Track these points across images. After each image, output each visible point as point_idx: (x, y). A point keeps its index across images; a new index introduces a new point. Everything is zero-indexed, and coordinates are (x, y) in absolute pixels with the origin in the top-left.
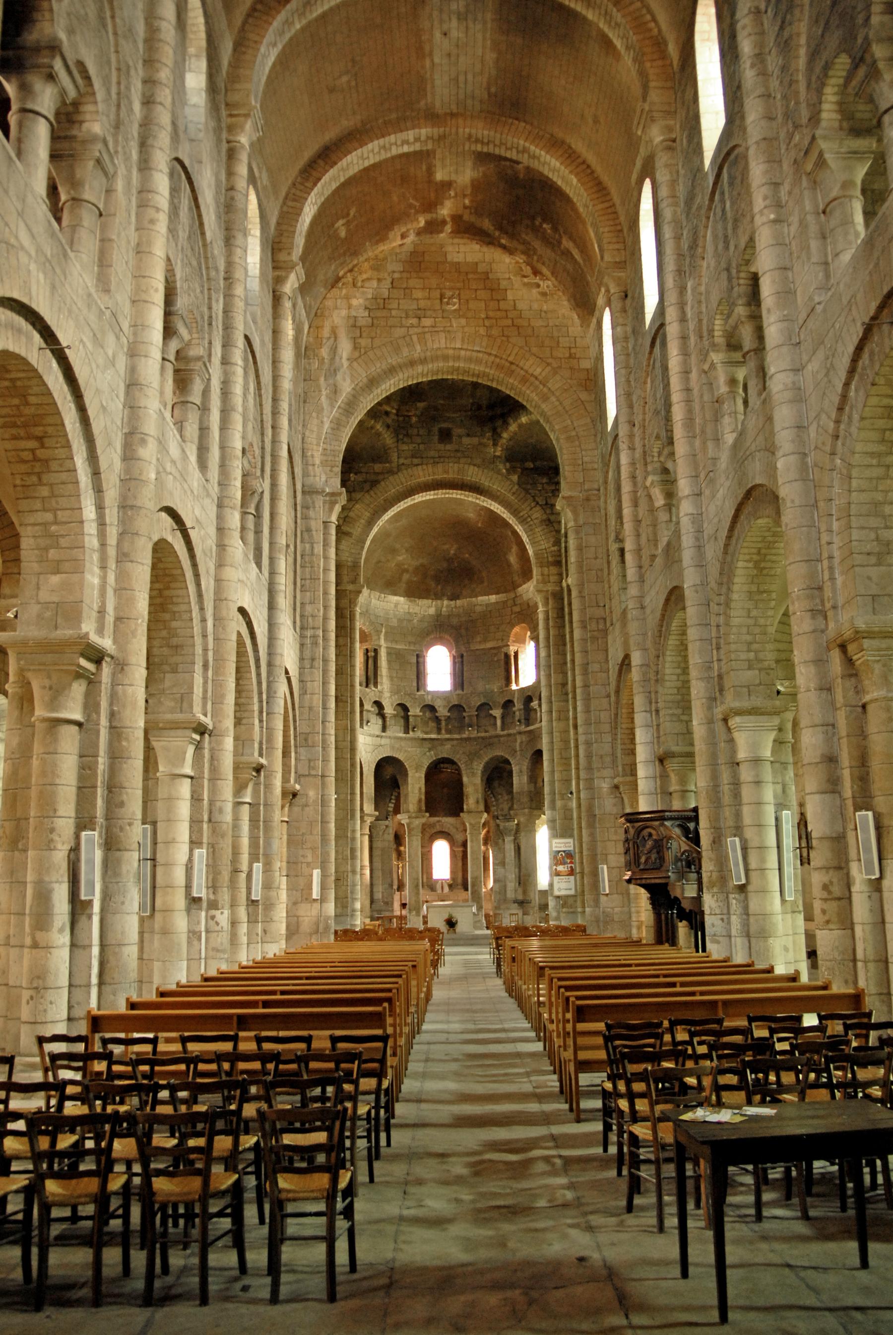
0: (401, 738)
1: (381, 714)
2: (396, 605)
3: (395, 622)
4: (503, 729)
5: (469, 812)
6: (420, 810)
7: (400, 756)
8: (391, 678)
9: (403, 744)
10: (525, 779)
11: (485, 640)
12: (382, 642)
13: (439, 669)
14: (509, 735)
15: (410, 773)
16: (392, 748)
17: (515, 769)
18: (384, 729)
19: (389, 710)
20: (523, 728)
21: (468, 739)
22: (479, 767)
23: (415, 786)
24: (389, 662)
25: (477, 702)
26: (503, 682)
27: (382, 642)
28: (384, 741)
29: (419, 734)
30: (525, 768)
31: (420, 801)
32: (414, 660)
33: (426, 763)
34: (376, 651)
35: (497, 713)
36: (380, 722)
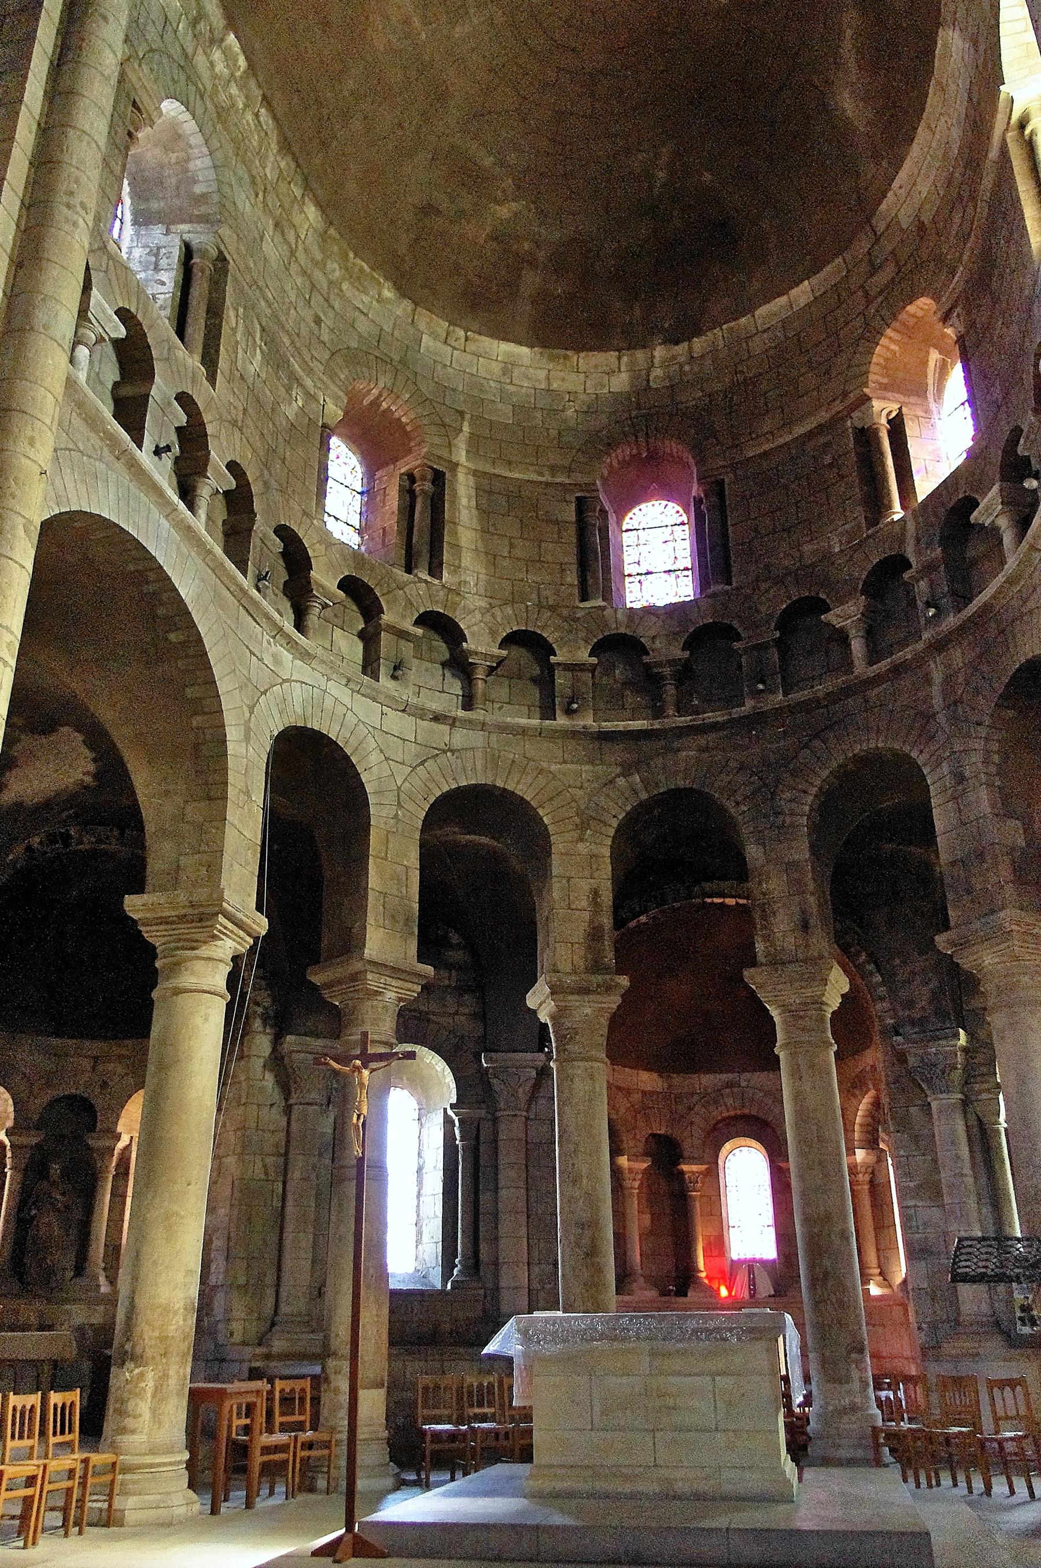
0: (524, 731)
1: (459, 664)
2: (508, 366)
3: (504, 413)
4: (874, 655)
5: (776, 962)
6: (596, 967)
7: (523, 787)
8: (492, 559)
9: (530, 748)
10: (982, 800)
11: (788, 424)
12: (461, 456)
13: (657, 555)
14: (897, 670)
15: (559, 844)
16: (493, 759)
17: (937, 782)
18: (468, 703)
19: (481, 643)
20: (951, 621)
21: (758, 718)
22: (801, 805)
23: (577, 885)
24: (485, 513)
25: (776, 602)
26: (860, 513)
27: (461, 456)
28: (460, 738)
29: (587, 721)
30: (974, 763)
31: (595, 934)
32: (570, 513)
33: (615, 813)
34: (438, 478)
35: (846, 615)
36: (456, 687)
